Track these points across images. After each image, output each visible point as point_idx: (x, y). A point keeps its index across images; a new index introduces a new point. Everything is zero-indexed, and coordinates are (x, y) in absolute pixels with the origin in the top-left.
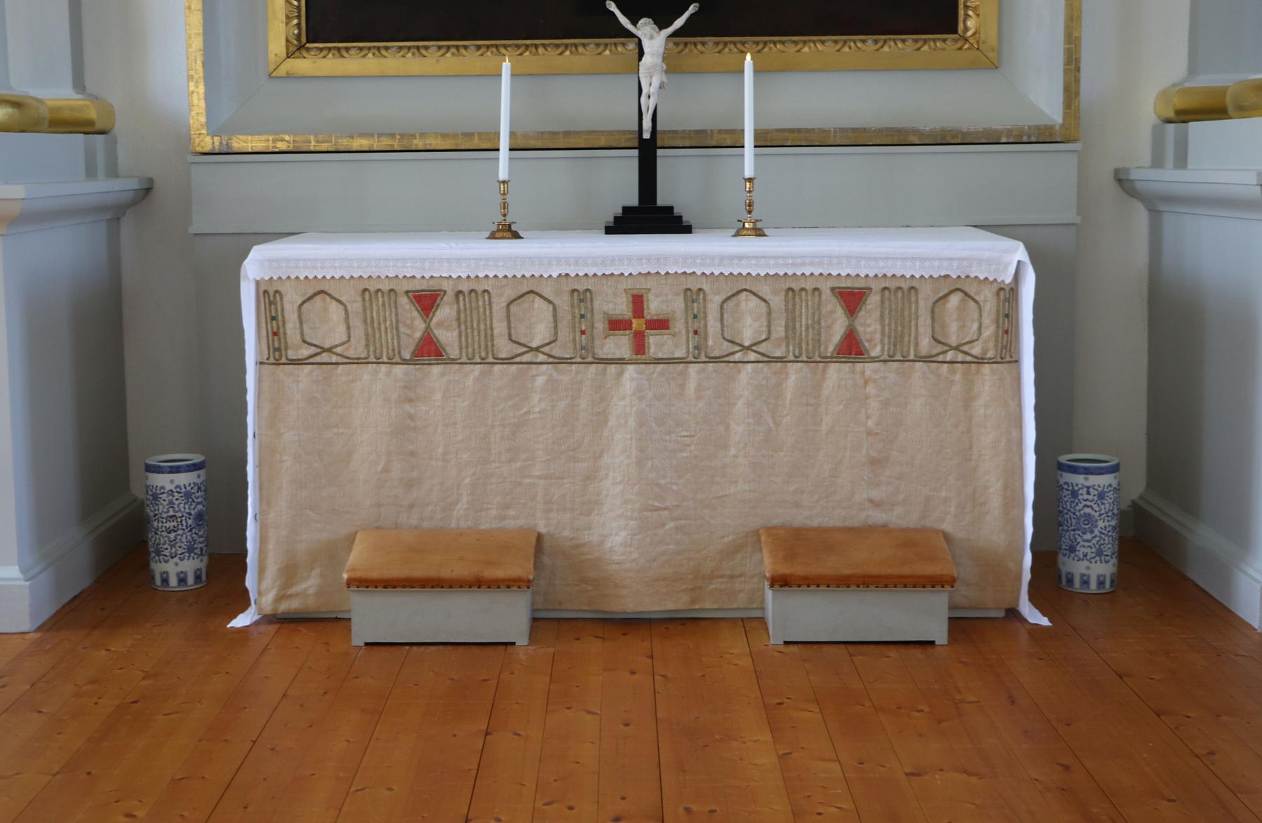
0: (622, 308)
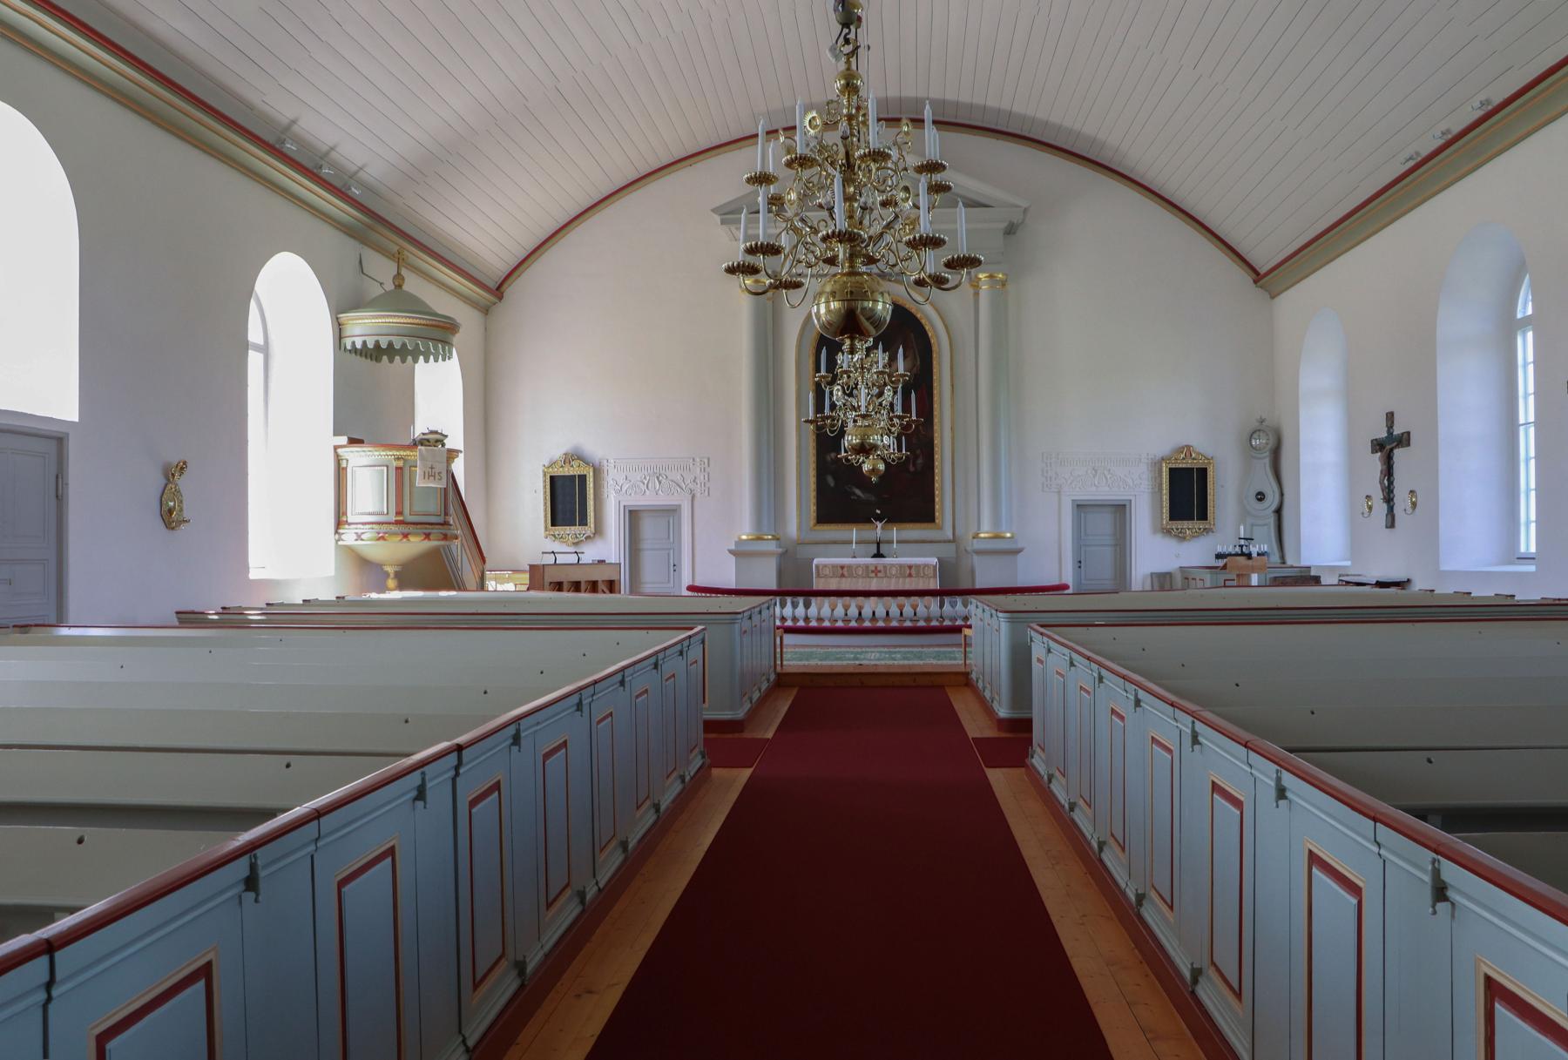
0: (874, 569)
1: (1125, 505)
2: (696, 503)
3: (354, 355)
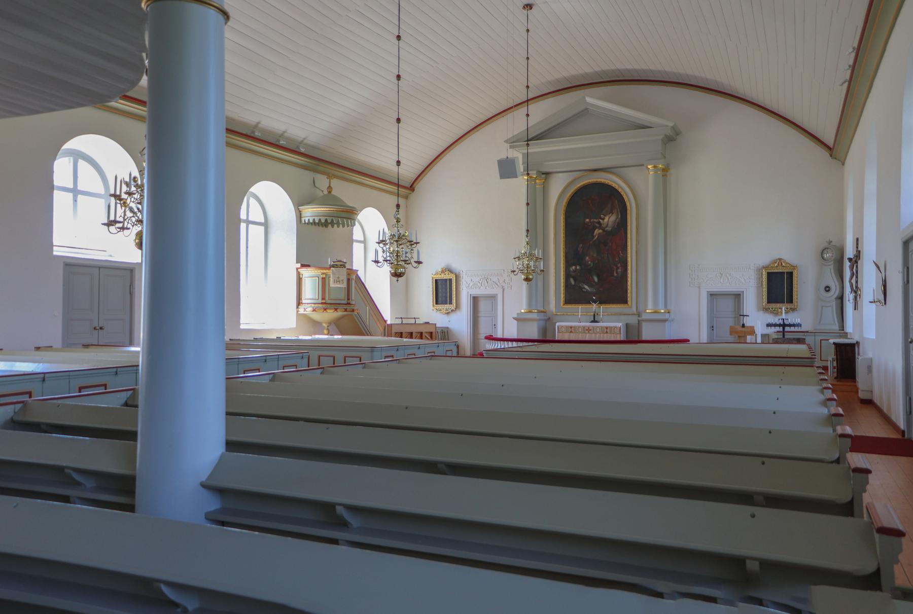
0: (587, 329)
1: (739, 295)
2: (505, 292)
3: (314, 226)
